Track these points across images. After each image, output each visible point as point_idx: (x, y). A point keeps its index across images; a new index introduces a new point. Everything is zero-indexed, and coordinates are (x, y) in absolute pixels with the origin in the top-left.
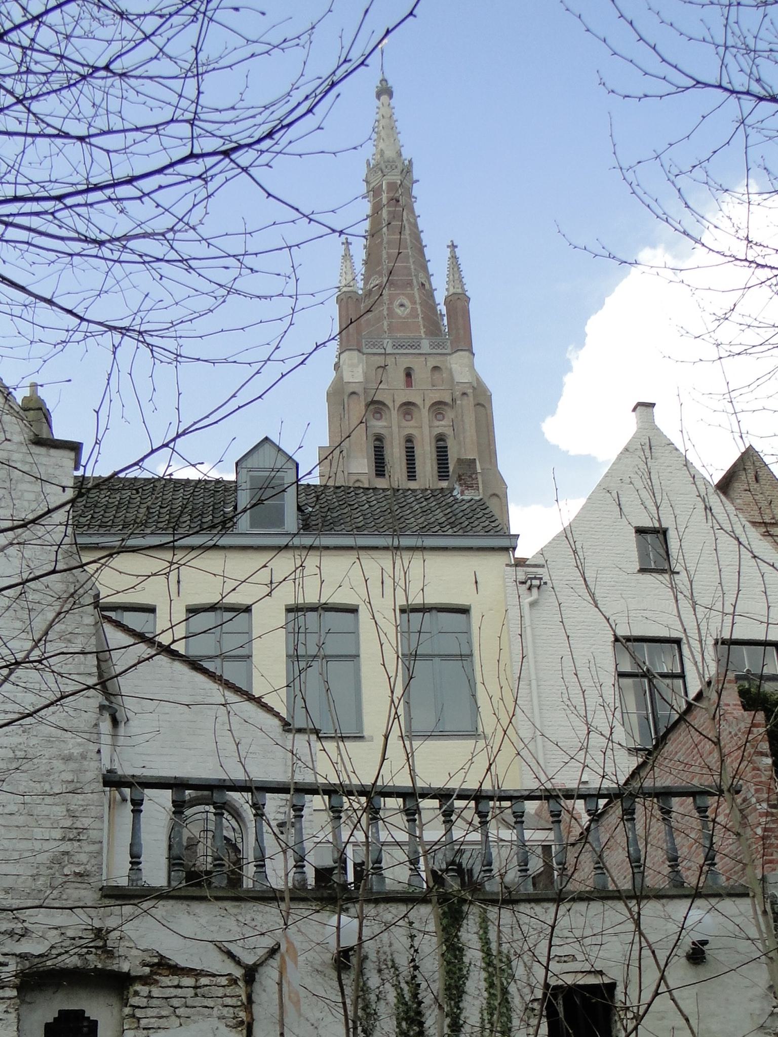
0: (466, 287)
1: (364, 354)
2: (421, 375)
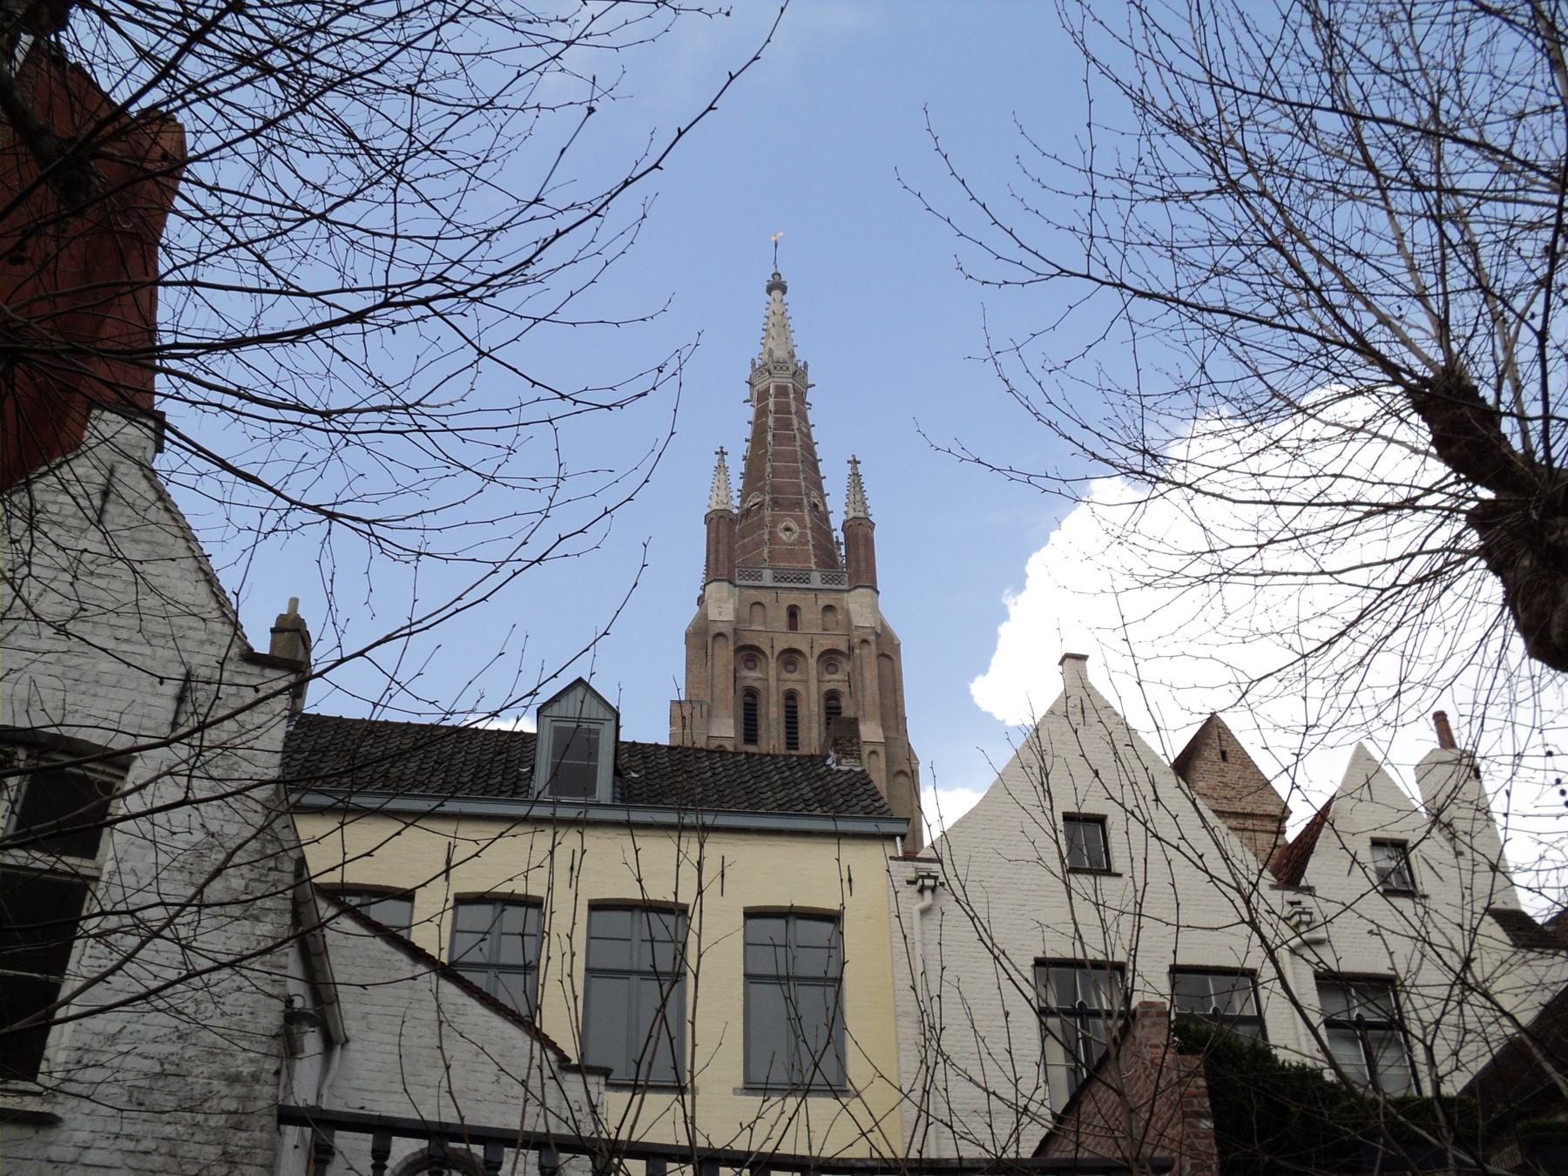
0: (870, 511)
1: (736, 586)
2: (810, 615)
